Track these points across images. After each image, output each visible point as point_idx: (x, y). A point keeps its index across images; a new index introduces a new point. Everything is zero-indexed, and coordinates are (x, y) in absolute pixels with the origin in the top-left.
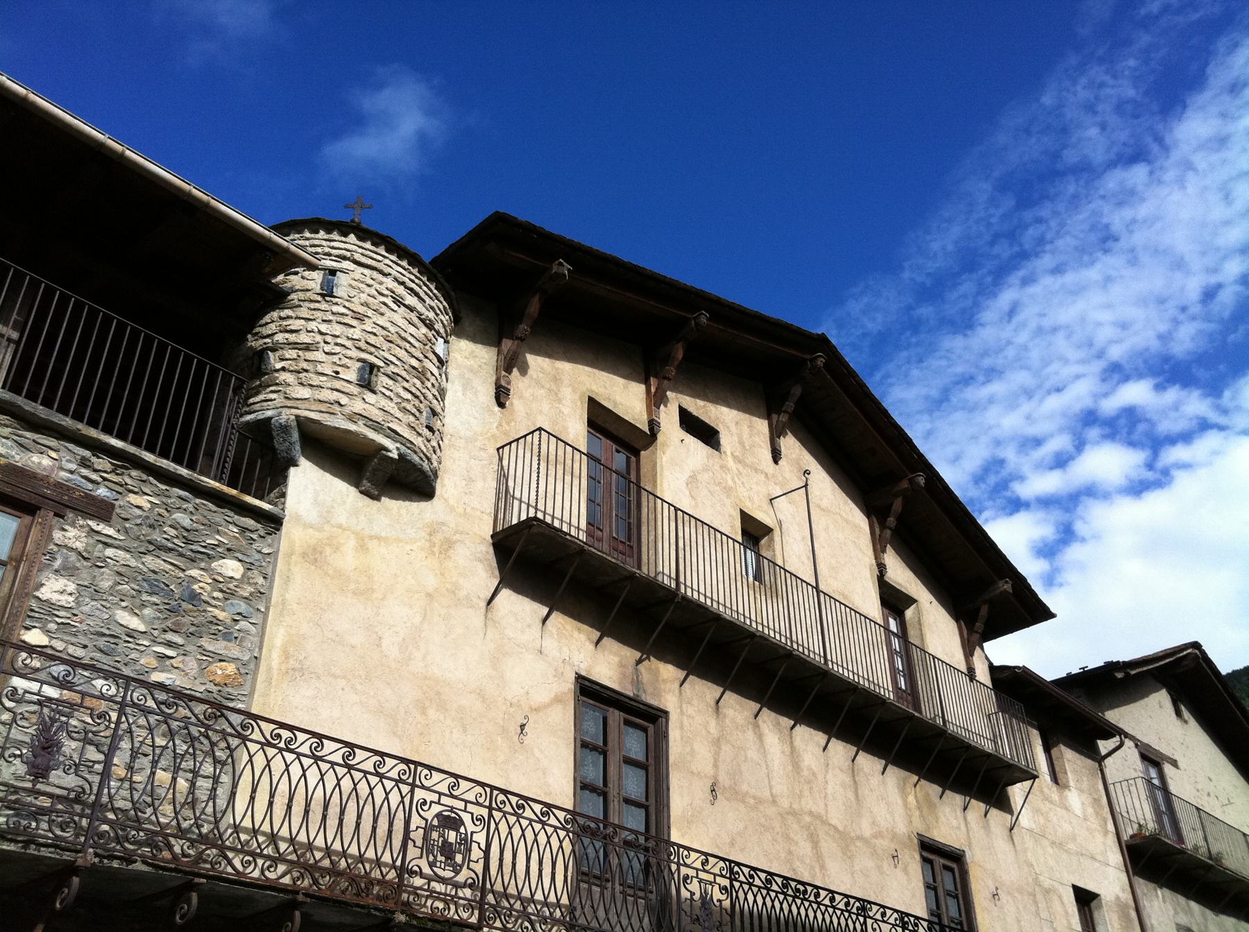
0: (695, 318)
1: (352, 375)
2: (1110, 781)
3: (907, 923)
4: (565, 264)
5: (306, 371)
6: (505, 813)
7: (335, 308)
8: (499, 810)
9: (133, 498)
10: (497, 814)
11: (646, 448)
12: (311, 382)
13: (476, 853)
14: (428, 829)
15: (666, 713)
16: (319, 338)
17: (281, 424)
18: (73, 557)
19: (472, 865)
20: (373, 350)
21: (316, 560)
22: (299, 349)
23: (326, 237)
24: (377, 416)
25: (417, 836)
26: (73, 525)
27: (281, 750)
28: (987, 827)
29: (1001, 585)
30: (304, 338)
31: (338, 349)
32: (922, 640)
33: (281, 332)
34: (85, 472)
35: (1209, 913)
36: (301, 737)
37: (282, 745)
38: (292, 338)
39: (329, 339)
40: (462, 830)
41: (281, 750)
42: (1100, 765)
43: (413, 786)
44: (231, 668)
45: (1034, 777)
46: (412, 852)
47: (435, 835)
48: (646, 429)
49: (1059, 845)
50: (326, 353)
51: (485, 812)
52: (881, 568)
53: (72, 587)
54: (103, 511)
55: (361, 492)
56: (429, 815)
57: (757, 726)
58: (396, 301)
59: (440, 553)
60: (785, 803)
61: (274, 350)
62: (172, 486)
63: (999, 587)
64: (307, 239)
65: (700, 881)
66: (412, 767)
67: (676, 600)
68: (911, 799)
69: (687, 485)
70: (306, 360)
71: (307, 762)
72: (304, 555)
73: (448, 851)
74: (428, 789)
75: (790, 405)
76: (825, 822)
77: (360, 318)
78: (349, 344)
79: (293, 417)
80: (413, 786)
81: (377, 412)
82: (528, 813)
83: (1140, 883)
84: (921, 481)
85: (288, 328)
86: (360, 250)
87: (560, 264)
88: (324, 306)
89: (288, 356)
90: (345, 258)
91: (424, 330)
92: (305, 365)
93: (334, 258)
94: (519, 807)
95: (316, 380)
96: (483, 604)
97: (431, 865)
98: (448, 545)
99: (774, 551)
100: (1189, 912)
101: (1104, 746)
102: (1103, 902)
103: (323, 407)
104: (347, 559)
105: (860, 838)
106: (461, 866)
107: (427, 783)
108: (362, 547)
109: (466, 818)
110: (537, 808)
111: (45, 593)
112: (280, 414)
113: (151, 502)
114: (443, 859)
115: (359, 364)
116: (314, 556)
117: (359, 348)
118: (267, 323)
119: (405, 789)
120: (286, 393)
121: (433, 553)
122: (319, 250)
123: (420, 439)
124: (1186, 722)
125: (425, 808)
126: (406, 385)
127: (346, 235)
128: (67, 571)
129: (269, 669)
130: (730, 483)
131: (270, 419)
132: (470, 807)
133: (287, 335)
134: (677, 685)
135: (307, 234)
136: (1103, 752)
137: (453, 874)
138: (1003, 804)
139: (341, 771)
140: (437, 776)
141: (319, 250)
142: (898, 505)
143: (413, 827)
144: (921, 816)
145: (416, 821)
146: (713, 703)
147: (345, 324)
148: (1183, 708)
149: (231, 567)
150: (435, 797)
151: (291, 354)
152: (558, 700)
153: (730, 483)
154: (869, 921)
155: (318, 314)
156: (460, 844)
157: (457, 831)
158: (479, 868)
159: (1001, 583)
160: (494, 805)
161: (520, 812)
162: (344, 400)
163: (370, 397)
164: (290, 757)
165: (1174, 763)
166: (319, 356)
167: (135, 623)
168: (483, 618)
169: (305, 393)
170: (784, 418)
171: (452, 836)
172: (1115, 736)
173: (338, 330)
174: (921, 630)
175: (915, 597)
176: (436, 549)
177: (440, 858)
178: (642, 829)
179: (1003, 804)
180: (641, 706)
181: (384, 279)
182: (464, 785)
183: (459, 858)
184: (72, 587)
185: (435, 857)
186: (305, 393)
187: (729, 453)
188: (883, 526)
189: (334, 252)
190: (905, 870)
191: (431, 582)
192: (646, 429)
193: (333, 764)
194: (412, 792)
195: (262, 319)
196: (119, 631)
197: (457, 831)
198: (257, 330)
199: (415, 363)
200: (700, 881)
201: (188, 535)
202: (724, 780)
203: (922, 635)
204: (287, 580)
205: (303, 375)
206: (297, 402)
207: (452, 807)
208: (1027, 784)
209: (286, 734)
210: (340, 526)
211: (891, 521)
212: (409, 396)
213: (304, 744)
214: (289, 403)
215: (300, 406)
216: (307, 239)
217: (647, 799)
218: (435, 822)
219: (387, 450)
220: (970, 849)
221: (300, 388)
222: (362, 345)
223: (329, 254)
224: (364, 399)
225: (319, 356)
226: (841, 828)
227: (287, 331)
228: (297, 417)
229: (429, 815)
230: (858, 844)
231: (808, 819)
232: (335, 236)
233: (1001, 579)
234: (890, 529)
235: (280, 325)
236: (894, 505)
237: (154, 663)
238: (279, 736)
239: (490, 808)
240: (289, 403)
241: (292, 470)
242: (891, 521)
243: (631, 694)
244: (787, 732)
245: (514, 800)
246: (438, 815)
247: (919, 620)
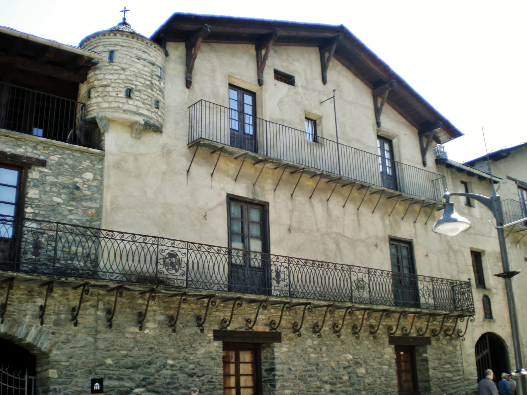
1: (123, 95)
3: (371, 272)
4: (208, 26)
6: (193, 250)
7: (115, 68)
8: (191, 249)
9: (52, 158)
10: (190, 251)
13: (183, 265)
14: (165, 258)
18: (36, 181)
19: (182, 269)
20: (130, 82)
21: (118, 167)
24: (134, 109)
25: (161, 261)
26: (34, 170)
27: (110, 239)
30: (105, 83)
31: (117, 85)
34: (35, 151)
36: (116, 234)
37: (110, 237)
39: (113, 81)
40: (178, 257)
41: (110, 239)
43: (158, 245)
44: (94, 211)
46: (160, 267)
47: (167, 260)
51: (186, 251)
53: (37, 192)
54: (43, 163)
56: (165, 254)
58: (138, 59)
59: (167, 156)
60: (323, 231)
65: (275, 265)
66: (157, 239)
68: (387, 222)
69: (278, 104)
71: (119, 242)
72: (114, 166)
73: (172, 265)
74: (163, 245)
76: (343, 236)
77: (124, 69)
78: (120, 81)
80: (158, 245)
81: (134, 107)
82: (203, 249)
88: (110, 67)
91: (151, 67)
92: (105, 93)
94: (199, 248)
96: (186, 173)
97: (167, 270)
98: (169, 152)
104: (131, 165)
106: (178, 269)
107: (163, 244)
108: (136, 159)
109: (179, 253)
110: (206, 247)
111: (30, 195)
113: (58, 157)
114: (171, 267)
116: (118, 166)
117: (125, 83)
119: (155, 246)
121: (164, 156)
122: (107, 43)
123: (153, 114)
125: (163, 252)
126: (145, 93)
128: (36, 186)
129: (106, 209)
130: (300, 99)
132: (180, 250)
134: (273, 191)
137: (175, 272)
139: (131, 243)
140: (167, 241)
143: (159, 259)
145: (160, 256)
146: (290, 196)
149: (89, 176)
150: (166, 248)
151: (100, 89)
152: (220, 204)
153: (300, 99)
154: (352, 273)
155: (108, 71)
156: (177, 262)
157: (176, 258)
158: (185, 269)
160: (189, 248)
161: (199, 249)
162: (121, 105)
163: (131, 102)
164: (113, 241)
167: (59, 200)
168: (186, 178)
169: (106, 105)
171: (174, 260)
173: (116, 77)
176: (165, 155)
177: (170, 267)
181: (133, 50)
182: (177, 243)
183: (177, 267)
184: (37, 192)
185: (168, 267)
187: (299, 85)
190: (381, 250)
191: (163, 167)
193: (128, 241)
194: (158, 247)
196: (54, 204)
197: (176, 258)
199: (148, 83)
200: (275, 265)
201: (73, 167)
202: (294, 225)
204: (109, 176)
207: (173, 251)
209: (111, 233)
210: (126, 153)
212: (146, 97)
213: (118, 236)
218: (167, 256)
220: (416, 238)
222: (126, 81)
226: (350, 237)
229: (165, 254)
230: (359, 242)
237: (68, 213)
238: (108, 235)
239: (188, 249)
241: (106, 135)
245: (197, 245)
246: (168, 254)
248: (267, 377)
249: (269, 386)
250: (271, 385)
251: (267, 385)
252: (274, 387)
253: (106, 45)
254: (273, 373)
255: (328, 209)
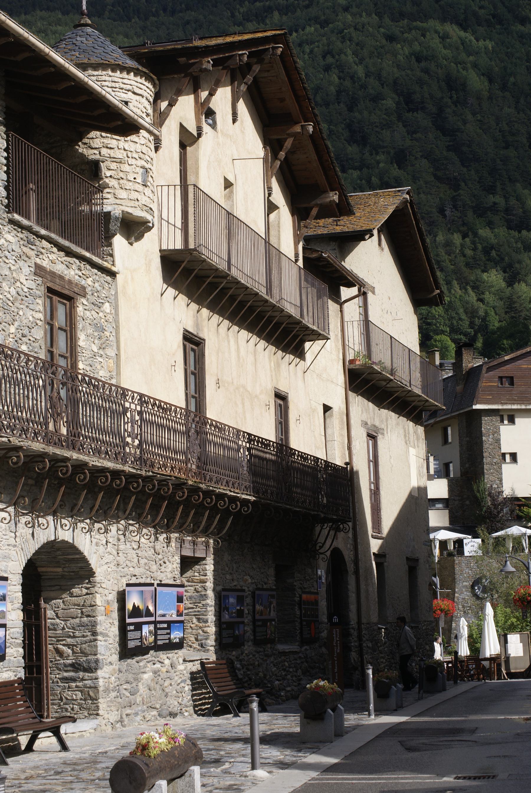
0: (240, 55)
2: (346, 319)
5: (122, 179)
11: (191, 145)
12: (126, 187)
15: (204, 340)
16: (125, 153)
17: (116, 216)
22: (117, 162)
23: (121, 76)
28: (296, 374)
29: (331, 195)
30: (120, 154)
32: (279, 239)
33: (104, 147)
35: (376, 408)
38: (112, 153)
39: (130, 155)
42: (341, 308)
45: (328, 339)
48: (195, 133)
49: (319, 376)
50: (129, 165)
52: (270, 191)
55: (129, 243)
57: (228, 336)
61: (103, 162)
62: (92, 268)
63: (329, 197)
64: (110, 76)
67: (228, 278)
68: (272, 363)
70: (121, 171)
75: (250, 78)
79: (121, 212)
83: (350, 393)
84: (311, 129)
85: (109, 146)
86: (136, 84)
87: (209, 62)
89: (112, 168)
90: (128, 91)
92: (121, 175)
93: (124, 91)
95: (129, 185)
99: (233, 201)
100: (367, 410)
101: (346, 292)
102: (334, 412)
103: (132, 204)
105: (256, 396)
112: (115, 209)
115: (142, 170)
118: (93, 138)
120: (114, 194)
122: (117, 85)
124: (382, 249)
127: (128, 73)
131: (110, 212)
133: (109, 151)
135: (110, 73)
136: (343, 298)
138: (300, 354)
141: (117, 85)
142: (288, 143)
144: (276, 375)
146: (216, 326)
147: (134, 142)
148: (383, 237)
151: (113, 166)
159: (331, 194)
165: (374, 293)
166: (125, 167)
170: (243, 88)
172: (355, 286)
174: (279, 231)
175: (279, 206)
178: (184, 407)
179: (300, 354)
180: (198, 339)
186: (123, 194)
188: (275, 156)
189: (124, 86)
190: (269, 413)
192: (195, 133)
195: (89, 133)
198: (86, 140)
203: (279, 235)
205: (121, 181)
206: (122, 201)
208: (321, 342)
211: (282, 154)
214: (118, 202)
215: (123, 204)
216: (110, 76)
217: (196, 393)
219: (149, 222)
221: (121, 191)
223: (122, 89)
224: (144, 193)
225: (125, 167)
227: (107, 148)
228: (123, 211)
231: (241, 390)
232: (124, 75)
233: (332, 190)
234: (280, 160)
235: (103, 143)
236: (287, 143)
240: (118, 202)
242: (282, 154)
243: (195, 333)
244: (236, 335)
247: (279, 223)
248: (193, 608)
249: (195, 620)
250: (199, 620)
251: (192, 619)
252: (206, 621)
253: (116, 88)
254: (204, 602)
255: (238, 345)
